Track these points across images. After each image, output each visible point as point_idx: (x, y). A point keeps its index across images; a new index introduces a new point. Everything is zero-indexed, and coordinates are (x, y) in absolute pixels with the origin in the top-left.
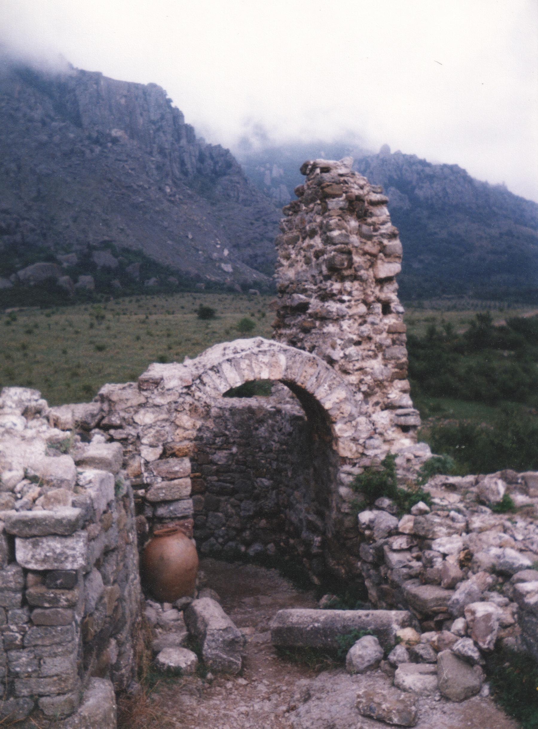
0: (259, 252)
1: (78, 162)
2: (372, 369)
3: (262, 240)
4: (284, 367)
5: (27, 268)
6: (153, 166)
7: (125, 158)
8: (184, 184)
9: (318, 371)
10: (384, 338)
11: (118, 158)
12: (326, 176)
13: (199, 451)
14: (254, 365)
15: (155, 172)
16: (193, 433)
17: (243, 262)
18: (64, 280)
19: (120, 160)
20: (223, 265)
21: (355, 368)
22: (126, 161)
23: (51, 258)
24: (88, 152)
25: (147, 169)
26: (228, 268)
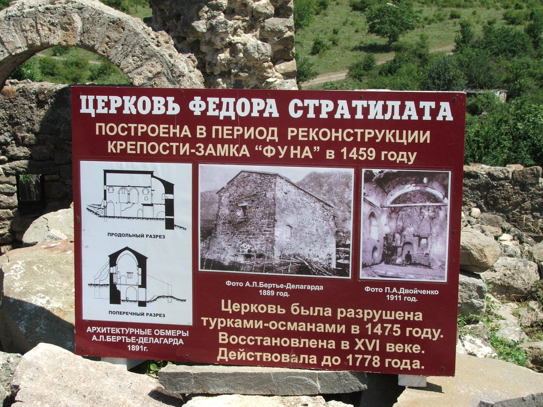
2: (244, 45)
4: (79, 30)
9: (124, 36)
13: (56, 148)
14: (39, 26)
21: (224, 43)
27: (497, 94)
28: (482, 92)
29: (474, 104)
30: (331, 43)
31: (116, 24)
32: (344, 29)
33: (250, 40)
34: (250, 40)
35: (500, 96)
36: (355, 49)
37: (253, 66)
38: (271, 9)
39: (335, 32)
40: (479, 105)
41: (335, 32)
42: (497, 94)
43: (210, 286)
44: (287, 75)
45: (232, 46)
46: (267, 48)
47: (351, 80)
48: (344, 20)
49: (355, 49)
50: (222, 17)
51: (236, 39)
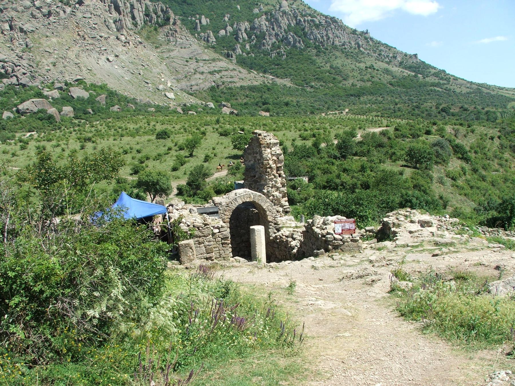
0: (193, 83)
1: (55, 21)
3: (195, 74)
5: (24, 104)
6: (112, 21)
7: (90, 16)
8: (135, 33)
10: (279, 185)
11: (84, 16)
12: (260, 137)
15: (113, 26)
16: (230, 217)
17: (182, 90)
18: (52, 111)
19: (85, 18)
20: (167, 94)
22: (91, 18)
23: (39, 95)
24: (62, 12)
25: (107, 23)
26: (171, 95)
27: (304, 179)
28: (296, 178)
29: (294, 185)
30: (213, 155)
31: (260, 196)
32: (218, 147)
33: (277, 194)
34: (277, 194)
35: (306, 179)
36: (227, 158)
37: (278, 200)
38: (281, 186)
39: (214, 149)
40: (296, 185)
41: (214, 149)
42: (304, 179)
43: (342, 230)
44: (286, 201)
45: (273, 196)
46: (281, 195)
47: (230, 176)
48: (216, 142)
49: (227, 158)
50: (270, 189)
51: (273, 194)
